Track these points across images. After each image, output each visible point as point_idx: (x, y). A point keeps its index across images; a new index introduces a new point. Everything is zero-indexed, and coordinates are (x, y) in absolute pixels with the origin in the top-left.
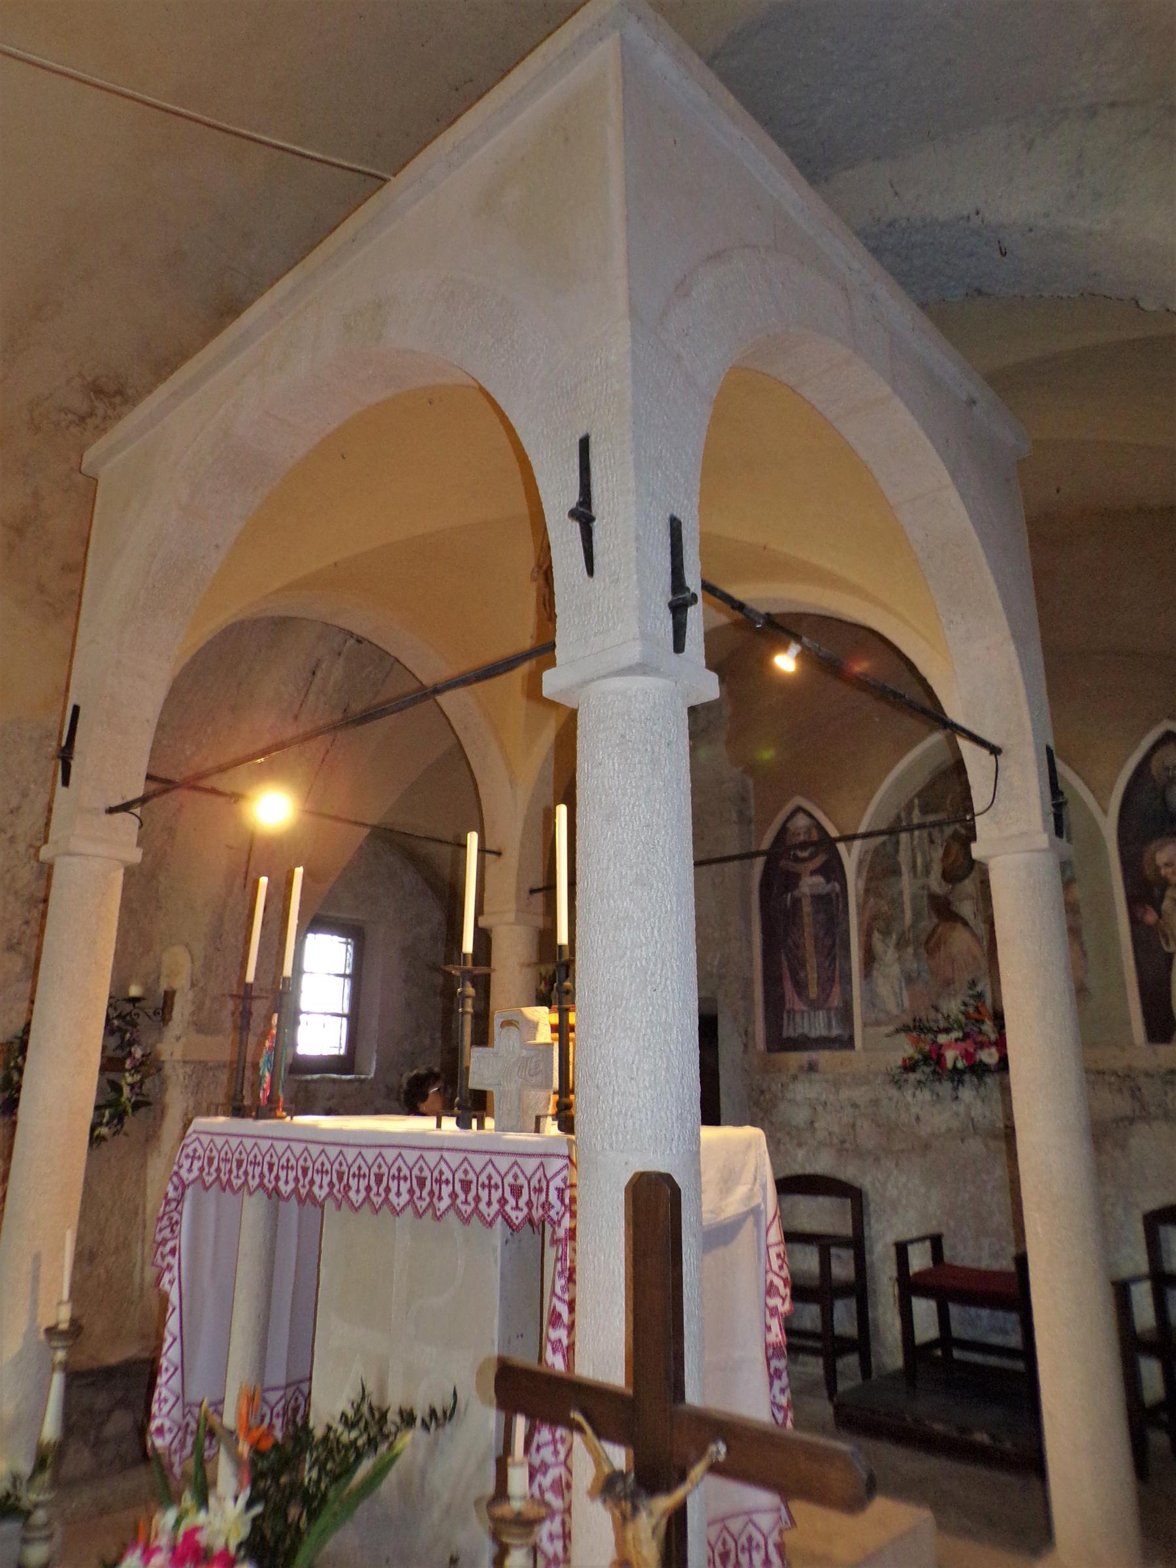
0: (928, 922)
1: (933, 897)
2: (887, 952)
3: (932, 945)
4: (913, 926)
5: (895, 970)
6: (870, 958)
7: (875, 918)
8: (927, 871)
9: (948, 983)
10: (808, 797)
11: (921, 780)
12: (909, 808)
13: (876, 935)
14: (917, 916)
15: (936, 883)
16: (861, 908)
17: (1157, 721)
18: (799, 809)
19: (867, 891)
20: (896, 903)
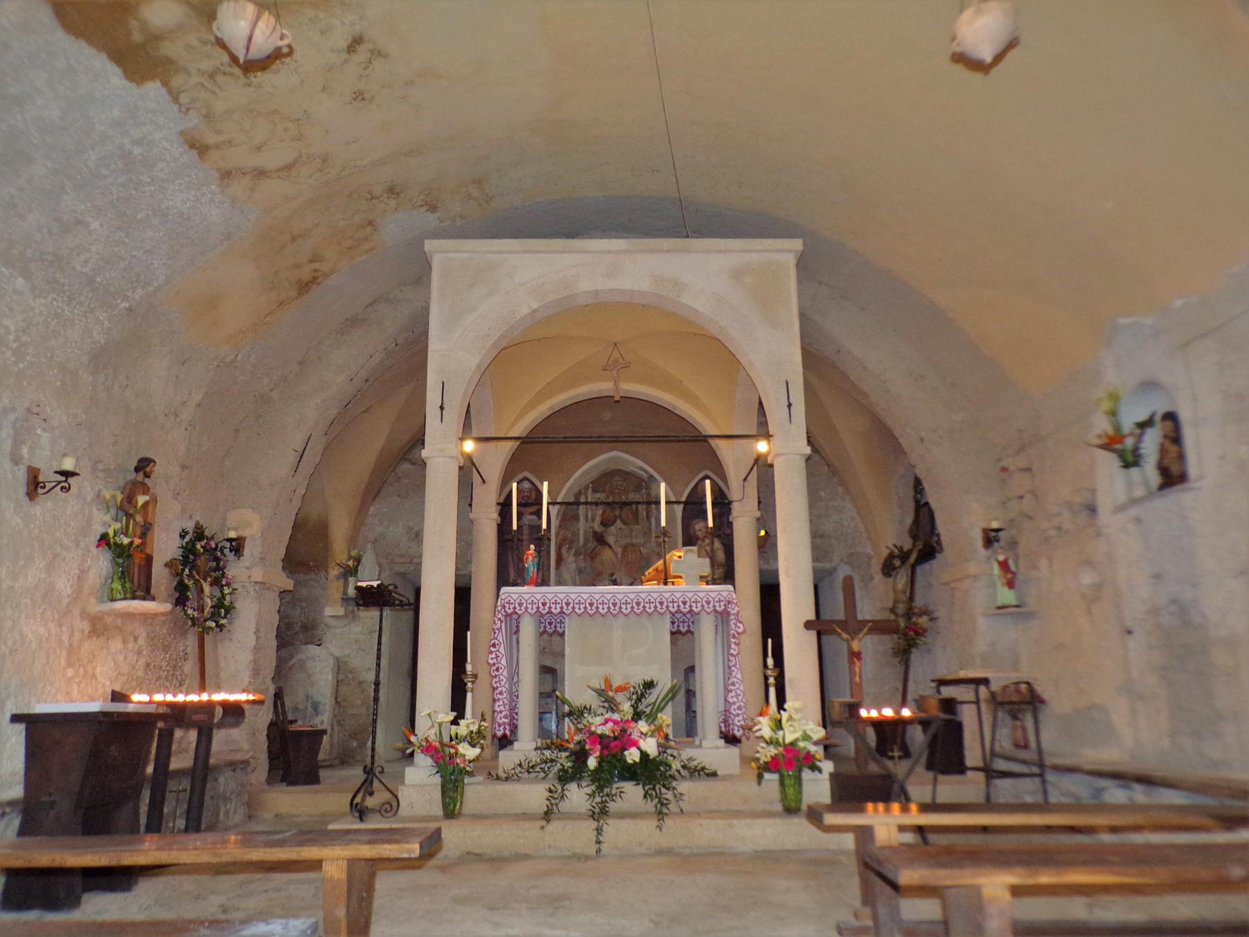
0: (592, 544)
1: (595, 533)
2: (570, 559)
3: (593, 556)
4: (584, 545)
5: (573, 566)
6: (560, 560)
7: (564, 540)
8: (593, 519)
9: (599, 574)
10: (533, 472)
11: (595, 475)
12: (587, 488)
13: (564, 550)
14: (586, 540)
15: (597, 526)
16: (557, 534)
17: (701, 470)
18: (526, 479)
19: (560, 526)
20: (576, 534)
